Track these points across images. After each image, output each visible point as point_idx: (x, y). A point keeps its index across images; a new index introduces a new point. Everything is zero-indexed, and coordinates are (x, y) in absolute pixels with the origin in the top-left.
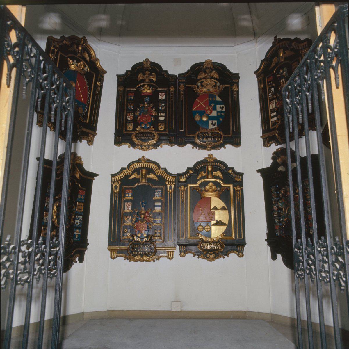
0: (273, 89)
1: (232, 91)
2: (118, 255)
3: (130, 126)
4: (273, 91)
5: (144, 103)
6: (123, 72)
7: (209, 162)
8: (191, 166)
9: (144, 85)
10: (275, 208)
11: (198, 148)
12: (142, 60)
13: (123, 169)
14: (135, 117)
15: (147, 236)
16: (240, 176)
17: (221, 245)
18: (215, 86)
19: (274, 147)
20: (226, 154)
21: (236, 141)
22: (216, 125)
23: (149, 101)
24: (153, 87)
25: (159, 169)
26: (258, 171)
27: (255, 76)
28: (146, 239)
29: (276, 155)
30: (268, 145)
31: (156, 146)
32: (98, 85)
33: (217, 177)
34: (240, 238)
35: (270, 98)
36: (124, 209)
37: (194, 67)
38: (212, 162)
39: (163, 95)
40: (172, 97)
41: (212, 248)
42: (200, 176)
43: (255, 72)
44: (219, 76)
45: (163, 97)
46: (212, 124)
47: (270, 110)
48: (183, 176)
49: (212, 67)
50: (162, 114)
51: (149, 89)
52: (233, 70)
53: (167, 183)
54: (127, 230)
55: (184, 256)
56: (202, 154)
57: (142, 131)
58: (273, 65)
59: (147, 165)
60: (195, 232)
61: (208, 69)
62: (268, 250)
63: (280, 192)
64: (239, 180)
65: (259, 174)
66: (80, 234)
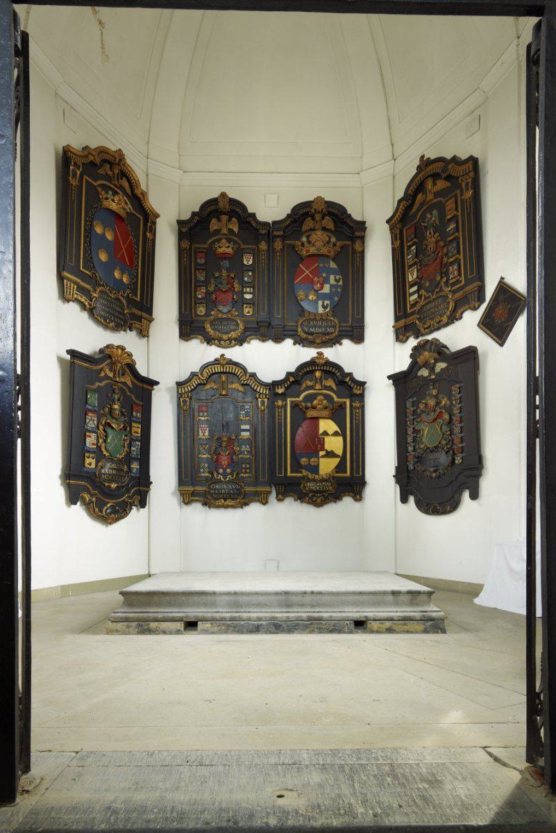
0: (414, 247)
1: (354, 252)
2: (192, 498)
3: (201, 309)
4: (415, 251)
5: (221, 271)
7: (318, 365)
8: (293, 370)
9: (221, 239)
10: (410, 430)
12: (215, 195)
13: (193, 375)
14: (208, 293)
15: (231, 474)
16: (360, 386)
17: (331, 485)
18: (328, 242)
19: (412, 342)
20: (343, 354)
21: (357, 336)
24: (235, 242)
25: (246, 375)
26: (389, 377)
27: (387, 226)
28: (230, 476)
29: (416, 351)
30: (404, 338)
31: (241, 341)
33: (329, 388)
35: (410, 263)
36: (198, 435)
37: (297, 209)
42: (304, 386)
43: (388, 222)
44: (336, 226)
46: (323, 306)
47: (409, 282)
49: (324, 210)
50: (248, 290)
51: (228, 247)
52: (357, 217)
53: (258, 395)
55: (282, 500)
56: (308, 354)
57: (220, 316)
58: (414, 210)
59: (228, 368)
60: (297, 466)
61: (319, 212)
63: (418, 407)
64: (358, 392)
65: (391, 381)
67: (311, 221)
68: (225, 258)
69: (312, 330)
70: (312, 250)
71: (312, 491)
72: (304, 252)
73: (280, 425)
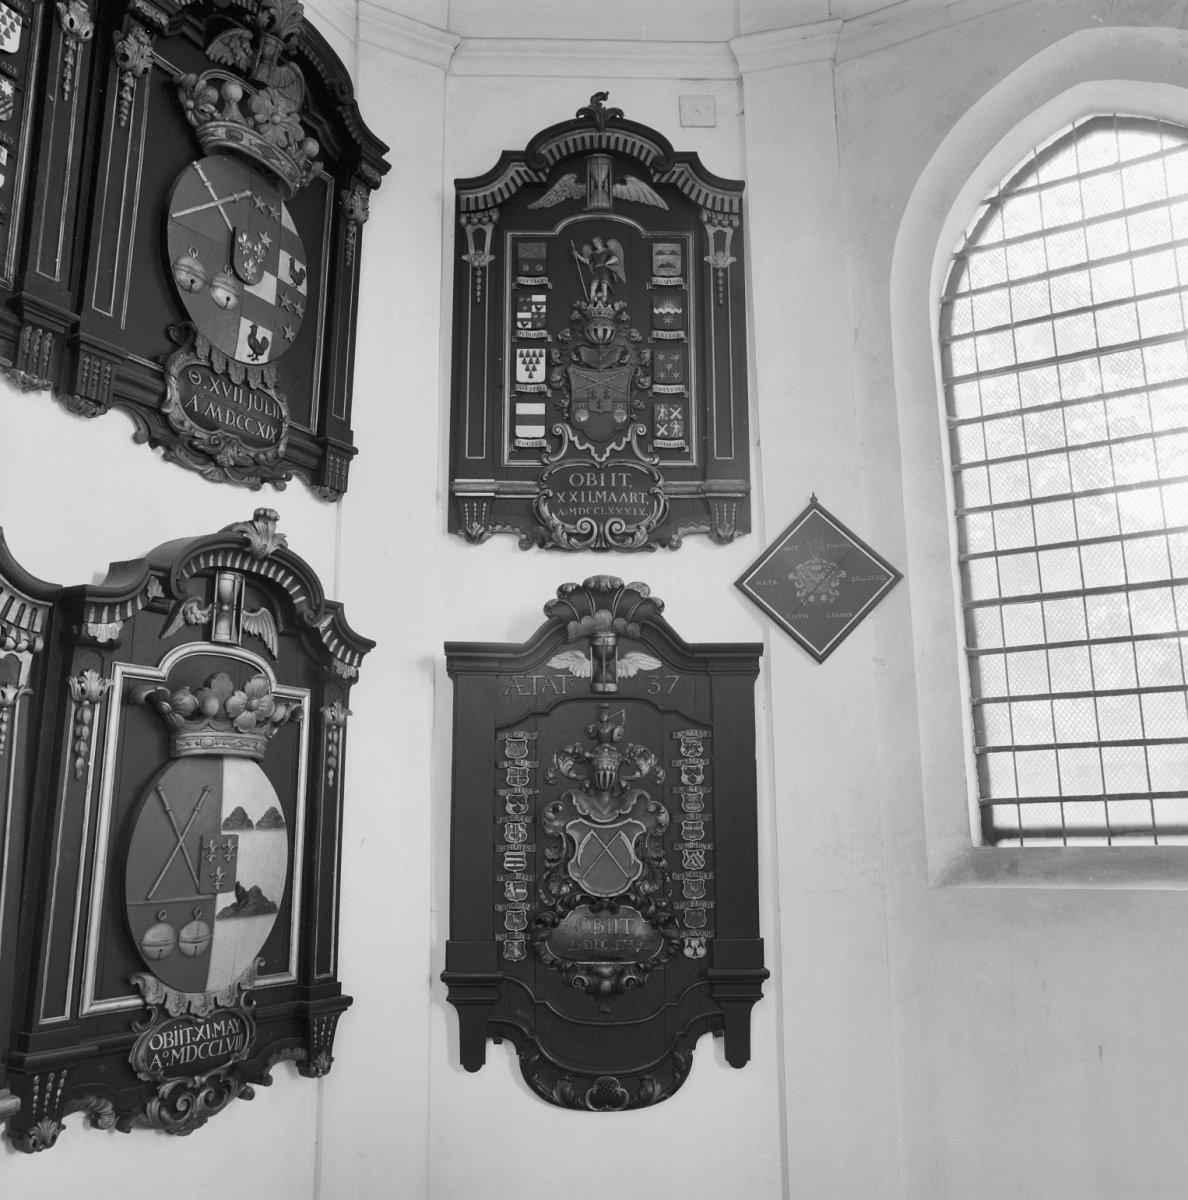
11: (161, 450)
22: (267, 352)
34: (323, 976)
38: (266, 558)
40: (69, 75)
41: (205, 1051)
48: (112, 607)
49: (294, 41)
61: (277, 34)
62: (441, 1024)
67: (247, 45)
69: (213, 411)
70: (248, 142)
71: (174, 1069)
72: (221, 133)
73: (78, 781)
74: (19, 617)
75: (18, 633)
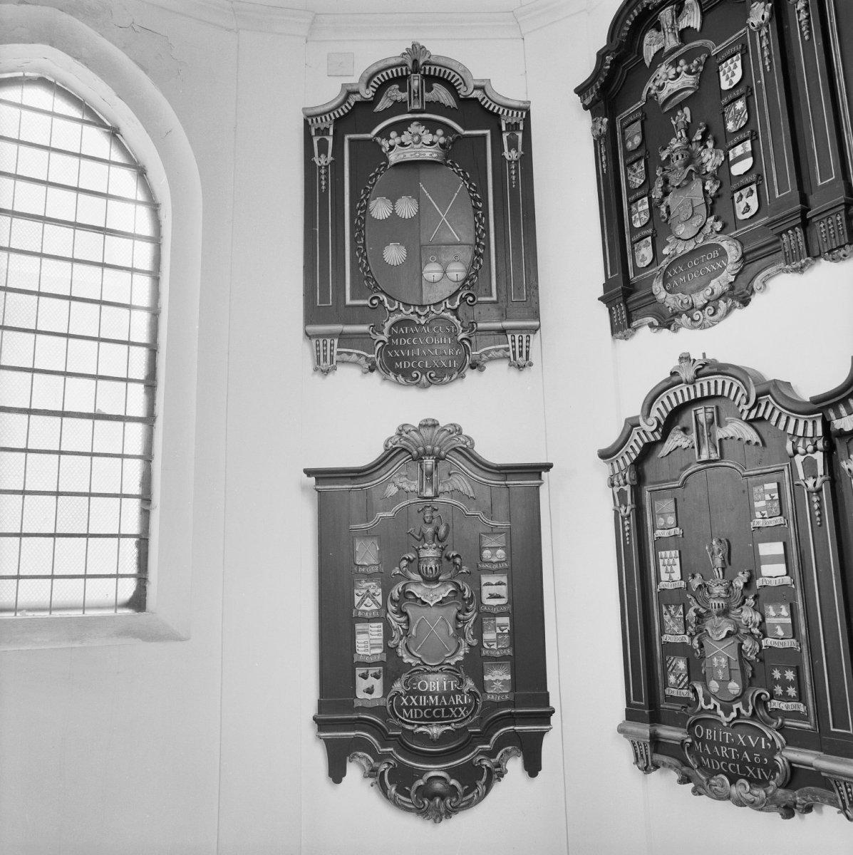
6: (584, 68)
23: (689, 120)
28: (739, 705)
31: (740, 295)
32: (510, 162)
36: (658, 580)
39: (732, 66)
45: (733, 74)
50: (739, 150)
51: (677, 75)
54: (673, 664)
66: (508, 677)
68: (680, 106)
74: (805, 430)
75: (804, 442)
